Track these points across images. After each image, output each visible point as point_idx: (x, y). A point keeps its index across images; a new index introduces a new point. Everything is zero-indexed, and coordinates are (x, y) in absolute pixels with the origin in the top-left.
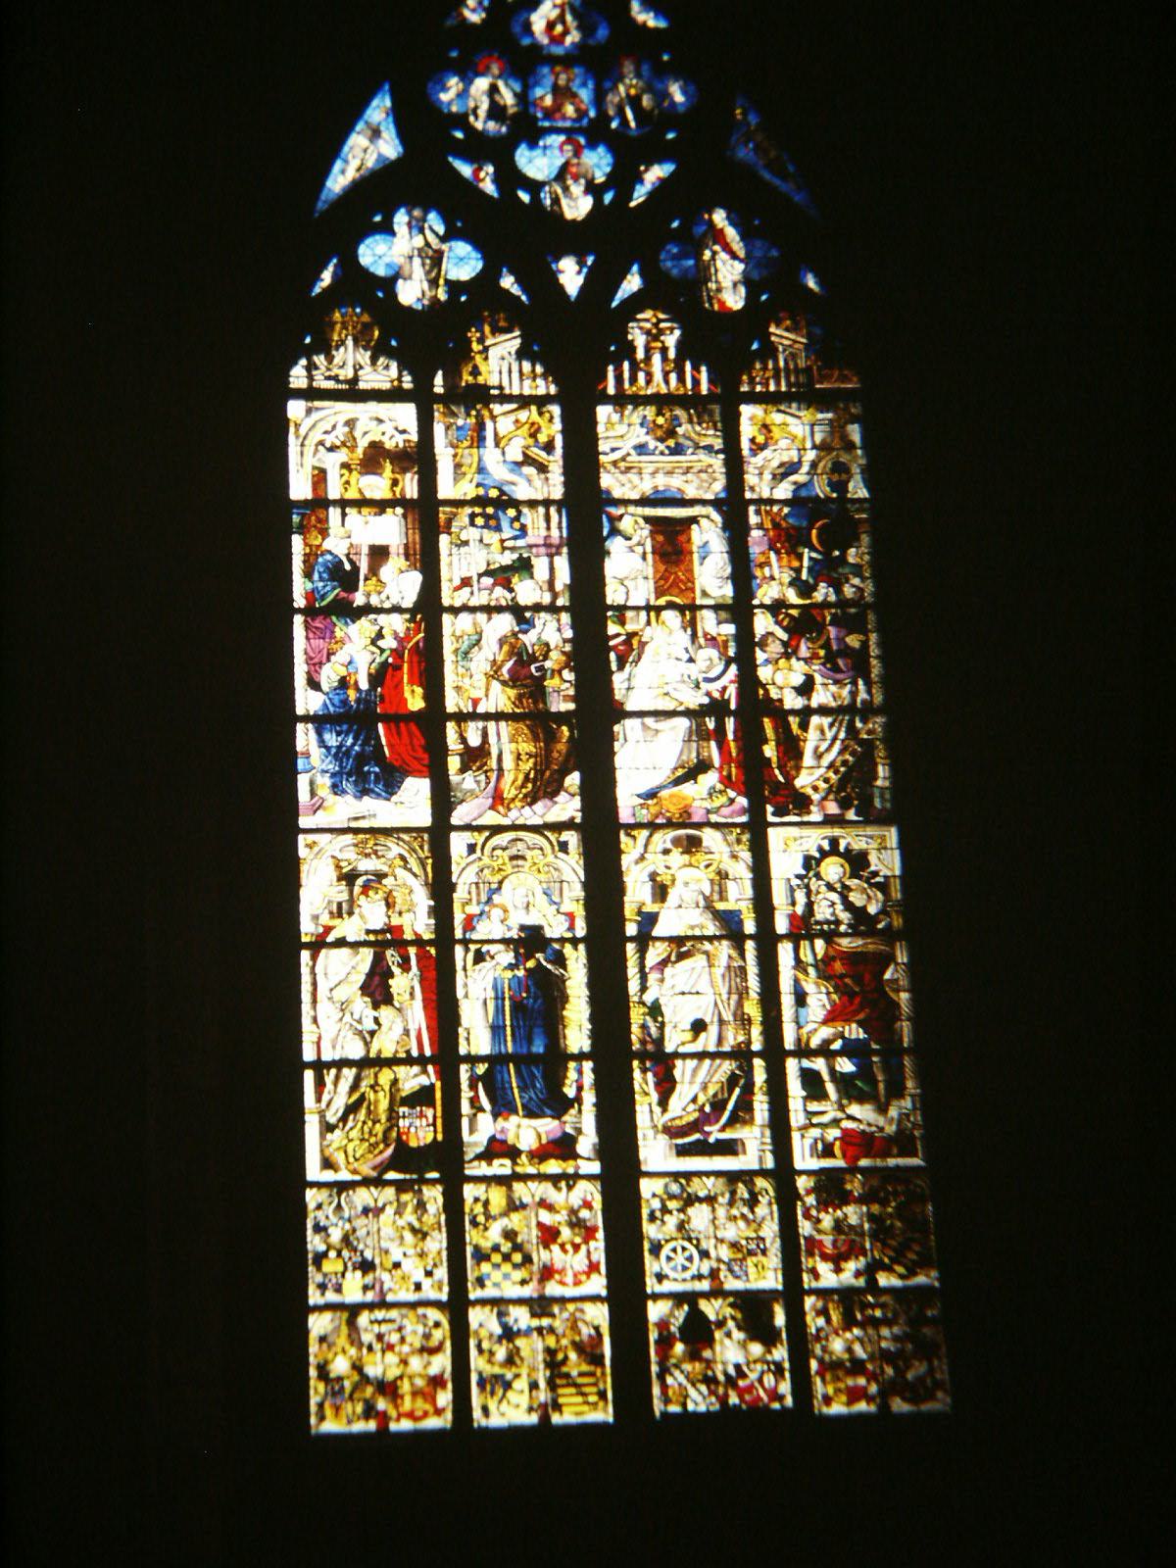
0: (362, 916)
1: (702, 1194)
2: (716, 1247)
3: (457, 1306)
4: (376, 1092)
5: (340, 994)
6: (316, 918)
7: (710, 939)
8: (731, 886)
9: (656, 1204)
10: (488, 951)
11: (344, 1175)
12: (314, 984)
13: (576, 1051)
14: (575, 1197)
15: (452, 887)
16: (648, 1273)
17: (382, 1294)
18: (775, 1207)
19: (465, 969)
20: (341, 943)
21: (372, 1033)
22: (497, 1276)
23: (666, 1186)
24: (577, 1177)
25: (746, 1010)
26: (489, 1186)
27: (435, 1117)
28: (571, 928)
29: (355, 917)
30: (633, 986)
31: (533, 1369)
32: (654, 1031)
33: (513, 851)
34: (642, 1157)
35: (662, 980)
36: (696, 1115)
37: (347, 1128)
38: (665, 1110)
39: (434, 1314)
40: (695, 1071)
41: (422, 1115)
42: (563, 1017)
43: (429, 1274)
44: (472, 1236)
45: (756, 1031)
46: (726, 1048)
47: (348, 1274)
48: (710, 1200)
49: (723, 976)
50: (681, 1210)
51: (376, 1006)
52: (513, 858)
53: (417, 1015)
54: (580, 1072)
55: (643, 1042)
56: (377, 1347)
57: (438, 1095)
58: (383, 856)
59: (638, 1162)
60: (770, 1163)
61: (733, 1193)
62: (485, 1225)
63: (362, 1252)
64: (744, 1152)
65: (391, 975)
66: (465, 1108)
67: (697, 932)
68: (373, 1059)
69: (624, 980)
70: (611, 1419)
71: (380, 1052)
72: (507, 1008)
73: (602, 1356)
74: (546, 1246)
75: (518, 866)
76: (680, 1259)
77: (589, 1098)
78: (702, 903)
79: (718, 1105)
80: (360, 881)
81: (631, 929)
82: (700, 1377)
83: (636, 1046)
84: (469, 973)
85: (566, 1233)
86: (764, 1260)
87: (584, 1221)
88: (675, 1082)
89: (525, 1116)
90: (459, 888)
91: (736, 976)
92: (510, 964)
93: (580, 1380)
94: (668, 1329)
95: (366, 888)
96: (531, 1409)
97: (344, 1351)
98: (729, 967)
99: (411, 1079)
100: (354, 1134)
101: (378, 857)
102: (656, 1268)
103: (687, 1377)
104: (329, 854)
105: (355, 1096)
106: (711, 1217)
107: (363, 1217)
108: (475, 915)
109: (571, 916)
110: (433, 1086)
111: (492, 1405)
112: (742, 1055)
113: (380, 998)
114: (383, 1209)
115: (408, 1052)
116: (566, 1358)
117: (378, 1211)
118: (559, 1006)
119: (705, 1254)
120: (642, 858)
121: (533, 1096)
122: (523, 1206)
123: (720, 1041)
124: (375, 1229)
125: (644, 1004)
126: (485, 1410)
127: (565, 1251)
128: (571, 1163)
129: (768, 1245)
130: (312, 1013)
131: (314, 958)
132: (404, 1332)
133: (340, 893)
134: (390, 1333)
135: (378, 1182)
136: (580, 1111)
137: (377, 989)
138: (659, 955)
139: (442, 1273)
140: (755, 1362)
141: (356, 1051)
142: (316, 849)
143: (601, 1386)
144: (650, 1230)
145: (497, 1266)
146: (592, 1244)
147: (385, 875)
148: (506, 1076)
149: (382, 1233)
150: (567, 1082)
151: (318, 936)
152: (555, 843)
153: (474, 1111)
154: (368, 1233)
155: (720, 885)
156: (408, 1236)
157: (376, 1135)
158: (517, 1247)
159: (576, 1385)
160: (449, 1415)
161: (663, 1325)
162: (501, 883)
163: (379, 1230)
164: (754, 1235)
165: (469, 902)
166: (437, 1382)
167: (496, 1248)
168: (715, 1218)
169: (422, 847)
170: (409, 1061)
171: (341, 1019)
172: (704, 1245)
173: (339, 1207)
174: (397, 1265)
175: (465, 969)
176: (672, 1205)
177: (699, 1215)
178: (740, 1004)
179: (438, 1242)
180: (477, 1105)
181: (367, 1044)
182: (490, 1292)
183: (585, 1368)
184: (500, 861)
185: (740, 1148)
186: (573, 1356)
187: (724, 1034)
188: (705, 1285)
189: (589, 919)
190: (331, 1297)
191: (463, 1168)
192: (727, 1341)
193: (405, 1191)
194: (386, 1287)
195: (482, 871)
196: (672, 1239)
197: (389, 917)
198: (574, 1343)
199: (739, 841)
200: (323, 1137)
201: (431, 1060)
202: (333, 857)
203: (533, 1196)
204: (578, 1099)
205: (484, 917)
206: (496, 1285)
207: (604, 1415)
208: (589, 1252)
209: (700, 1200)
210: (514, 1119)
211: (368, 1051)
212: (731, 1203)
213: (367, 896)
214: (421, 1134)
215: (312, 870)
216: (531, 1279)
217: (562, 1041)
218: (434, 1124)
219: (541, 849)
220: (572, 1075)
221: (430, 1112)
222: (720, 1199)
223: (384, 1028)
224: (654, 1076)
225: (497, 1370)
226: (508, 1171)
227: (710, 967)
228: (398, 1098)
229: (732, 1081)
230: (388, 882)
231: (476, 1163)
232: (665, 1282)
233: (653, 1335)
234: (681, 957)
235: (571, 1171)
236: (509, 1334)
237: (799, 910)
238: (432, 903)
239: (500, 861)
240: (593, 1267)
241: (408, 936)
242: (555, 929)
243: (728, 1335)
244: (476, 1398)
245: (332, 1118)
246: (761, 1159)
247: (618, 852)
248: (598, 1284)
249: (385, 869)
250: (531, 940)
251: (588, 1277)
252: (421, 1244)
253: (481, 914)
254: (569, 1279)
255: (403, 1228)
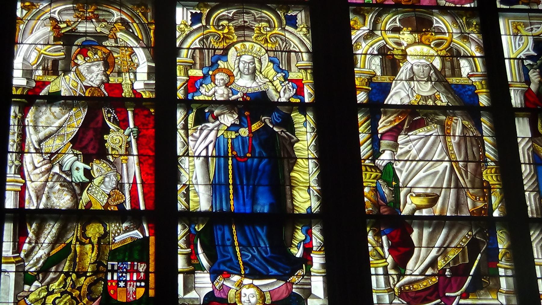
0: (79, 74)
4: (82, 244)
5: (52, 145)
6: (28, 73)
7: (443, 110)
8: (463, 63)
10: (212, 112)
12: (23, 136)
13: (303, 211)
15: (176, 52)
19: (185, 127)
20: (54, 99)
21: (83, 186)
25: (485, 178)
27: (147, 272)
28: (299, 92)
29: (72, 75)
30: (365, 150)
32: (386, 191)
33: (240, 22)
35: (395, 146)
36: (435, 280)
37: (48, 279)
38: (401, 275)
40: (432, 238)
41: (132, 271)
42: (290, 178)
45: (495, 200)
46: (465, 213)
49: (459, 144)
51: (87, 160)
52: (237, 28)
53: (132, 168)
54: (309, 233)
55: (376, 205)
57: (152, 250)
58: (104, 20)
65: (107, 130)
66: (181, 263)
67: (430, 103)
68: (81, 210)
69: (358, 145)
71: (89, 204)
72: (230, 167)
75: (244, 36)
77: (317, 260)
78: (434, 77)
79: (459, 271)
80: (79, 42)
81: (361, 97)
83: (369, 208)
84: (190, 132)
88: (412, 247)
89: (246, 276)
90: (184, 53)
91: (472, 145)
92: (233, 125)
95: (83, 51)
98: (463, 137)
99: (123, 235)
100: (54, 286)
101: (99, 21)
104: (47, 15)
105: (59, 248)
108: (198, 78)
109: (299, 85)
110: (146, 240)
112: (482, 221)
113: (90, 151)
115: (121, 206)
118: (286, 169)
120: (371, 34)
121: (256, 254)
123: (458, 205)
125: (376, 167)
130: (17, 163)
131: (24, 111)
133: (57, 52)
136: (309, 273)
137: (90, 144)
138: (391, 122)
141: (63, 201)
142: (34, 11)
147: (106, 38)
148: (227, 235)
150: (295, 242)
151: (30, 90)
152: (283, 18)
153: (191, 268)
155: (452, 62)
157: (80, 289)
162: (226, 50)
165: (193, 66)
169: (145, 15)
170: (120, 215)
171: (49, 170)
175: (185, 127)
178: (477, 173)
180: (195, 262)
181: (76, 197)
184: (226, 31)
187: (462, 200)
189: (317, 86)
195: (207, 38)
197: (107, 76)
199: (469, 25)
200: (18, 287)
201: (147, 216)
202: (51, 18)
204: (307, 259)
205: (208, 79)
210: (236, 278)
211: (77, 203)
213: (85, 56)
214: (131, 289)
215: (29, 30)
217: (289, 201)
218: (146, 280)
219: (268, 21)
220: (300, 236)
221: (142, 268)
223: (96, 182)
224: (388, 239)
227: (445, 136)
228: (107, 252)
229: (473, 247)
230: (109, 43)
234: (414, 126)
237: (533, 87)
238: (153, 65)
239: (226, 31)
241: (127, 93)
242: (282, 94)
245: (30, 266)
247: (349, 29)
249: (106, 32)
250: (254, 106)
253: (205, 77)
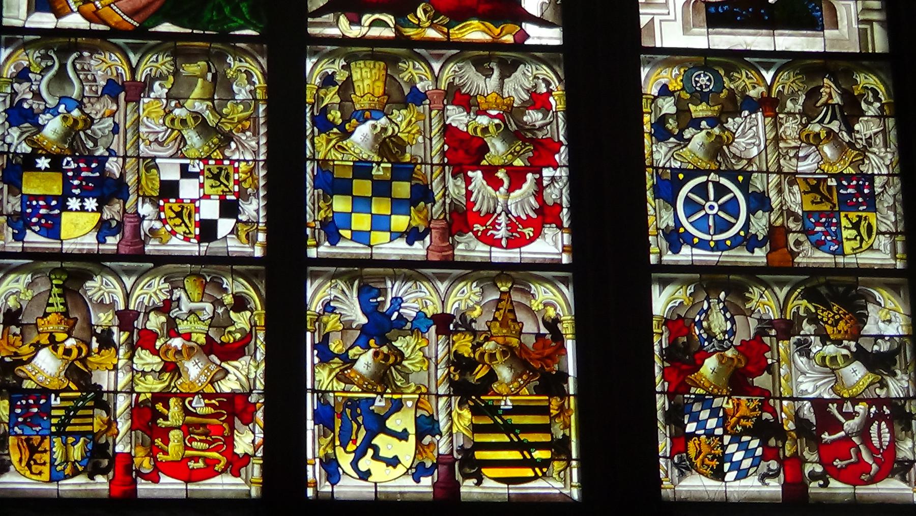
1: (752, 93)
2: (780, 192)
3: (283, 270)
9: (668, 106)
11: (74, 21)
14: (518, 85)
16: (652, 230)
17: (138, 240)
18: (891, 122)
22: (361, 222)
23: (687, 79)
24: (518, 54)
26: (351, 58)
31: (424, 394)
34: (644, 20)
39: (235, 286)
43: (229, 209)
44: (320, 146)
47: (74, 203)
48: (769, 105)
50: (714, 121)
56: (120, 337)
59: (635, 30)
60: (879, 42)
61: (813, 94)
62: (341, 127)
63: (102, 160)
64: (835, 25)
70: (575, 494)
73: (564, 376)
74: (460, 171)
76: (712, 208)
82: (749, 424)
85: (497, 149)
86: (872, 218)
87: (533, 129)
93: (516, 420)
94: (689, 334)
96: (418, 471)
97: (54, 344)
102: (667, 220)
103: (723, 422)
106: (771, 135)
107: (106, 99)
111: (345, 460)
114: (146, 87)
116: (492, 377)
117: (135, 91)
119: (759, 202)
122: (417, 97)
124: (131, 119)
126: (331, 467)
127: (496, 184)
128: (509, 27)
129: (878, 190)
132: (174, 313)
134: (147, 314)
135: (139, 37)
139: (253, 208)
140: (855, 401)
143: (558, 432)
144: (659, 154)
145: (361, 204)
146: (547, 172)
149: (143, 129)
154: (115, 130)
156: (193, 138)
158: (403, 171)
159: (508, 429)
160: (256, 470)
161: (677, 323)
163: (137, 123)
164: (851, 170)
166: (235, 407)
167: (362, 169)
168: (777, 139)
172: (758, 183)
173: (61, 77)
174: (169, 189)
176: (699, 110)
177: (750, 136)
179: (249, 151)
182: (347, 248)
183: (526, 397)
185: (826, 20)
186: (505, 373)
188: (760, 256)
190: (34, 239)
191: (305, 25)
192: (801, 361)
193: (191, 57)
194: (146, 225)
196: (697, 172)
198: (508, 350)
203: (436, 79)
206: (360, 237)
207: (561, 483)
208: (539, 182)
209: (753, 105)
212: (808, 113)
216: (428, 230)
222: (789, 104)
225: (355, 392)
226: (389, 33)
231: (329, 17)
232: (686, 250)
233: (660, 341)
235: (509, 39)
236: (381, 327)
240: (546, 215)
243: (804, 349)
244: (314, 445)
246: (863, 34)
248: (550, 245)
251: (537, 234)
252: (217, 155)
254: (502, 233)
255: (183, 122)
